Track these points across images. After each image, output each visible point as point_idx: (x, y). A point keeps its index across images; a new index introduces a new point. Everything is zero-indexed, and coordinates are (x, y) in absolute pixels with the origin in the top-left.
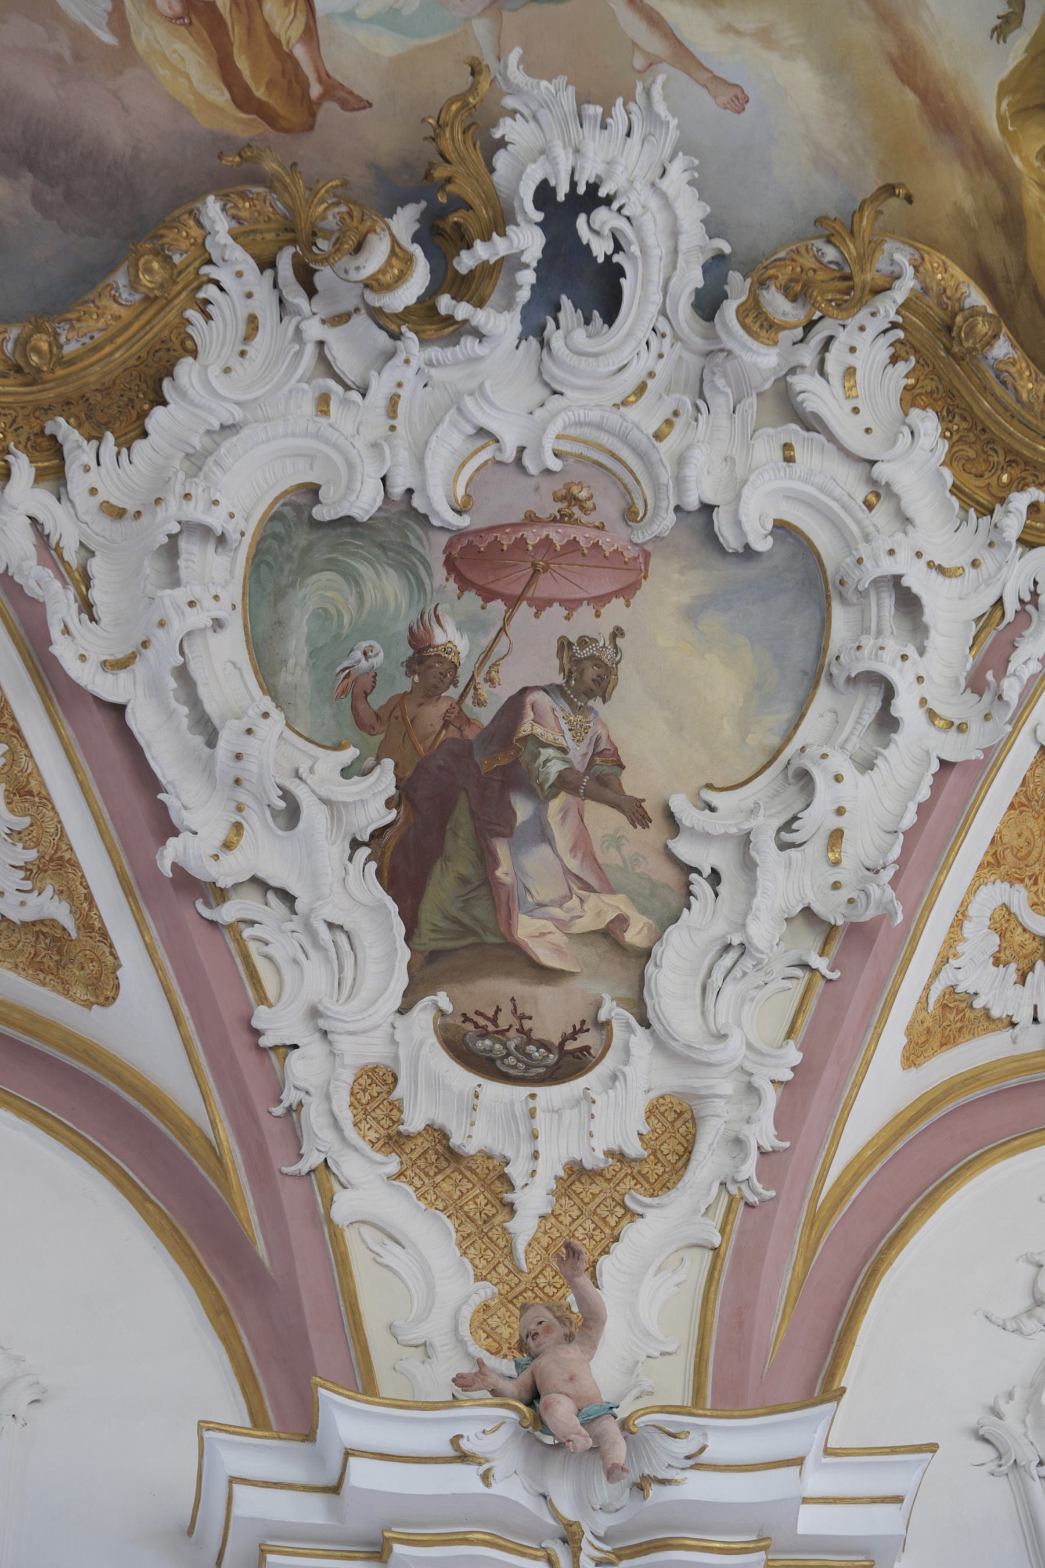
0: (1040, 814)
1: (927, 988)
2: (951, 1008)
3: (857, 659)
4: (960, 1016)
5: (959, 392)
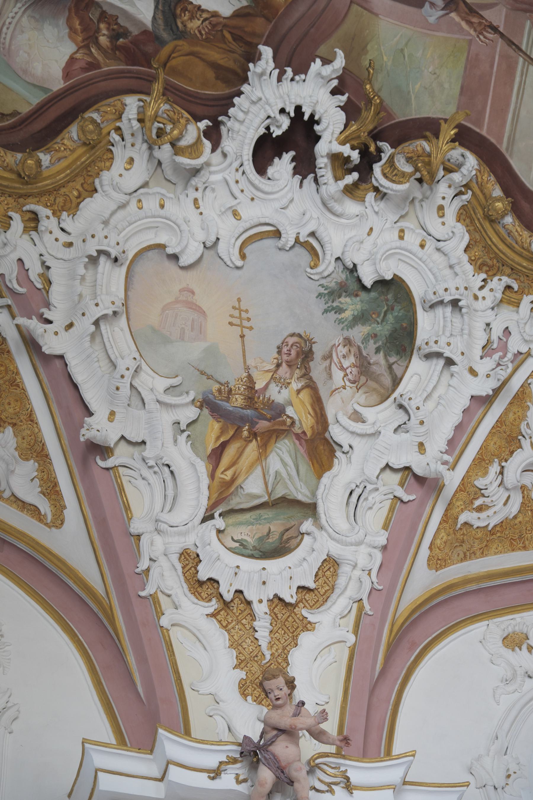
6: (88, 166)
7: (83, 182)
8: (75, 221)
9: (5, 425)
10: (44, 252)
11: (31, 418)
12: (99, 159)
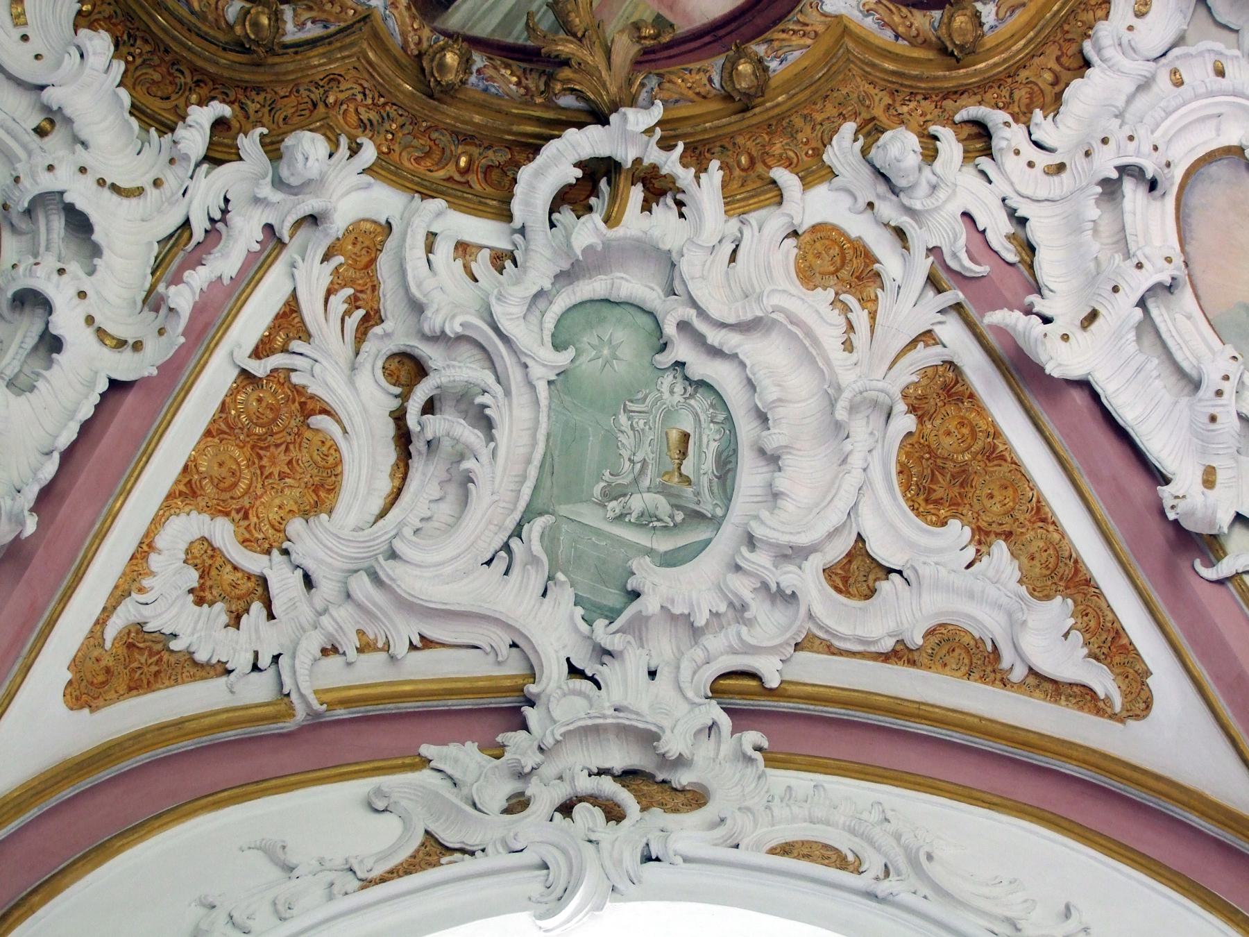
0: (245, 443)
1: (101, 622)
2: (138, 647)
3: (14, 279)
4: (154, 659)
5: (135, 12)
6: (1065, 22)
7: (1059, 53)
8: (1060, 125)
9: (988, 540)
10: (1008, 192)
11: (1041, 515)
12: (1082, 6)
